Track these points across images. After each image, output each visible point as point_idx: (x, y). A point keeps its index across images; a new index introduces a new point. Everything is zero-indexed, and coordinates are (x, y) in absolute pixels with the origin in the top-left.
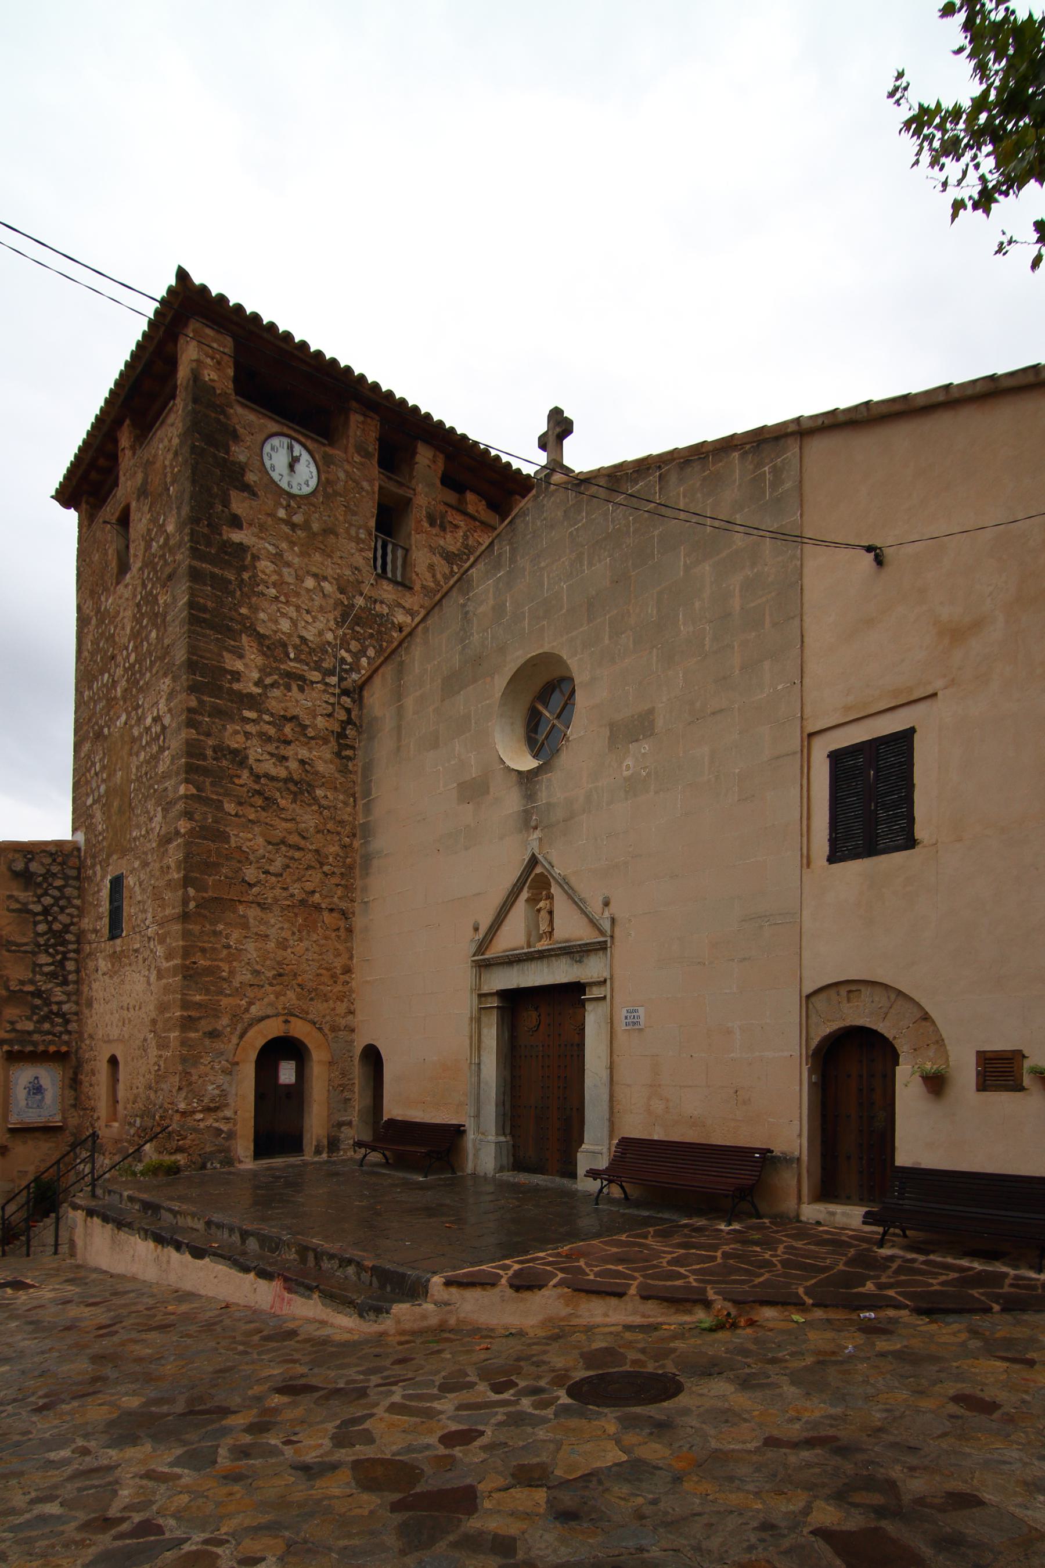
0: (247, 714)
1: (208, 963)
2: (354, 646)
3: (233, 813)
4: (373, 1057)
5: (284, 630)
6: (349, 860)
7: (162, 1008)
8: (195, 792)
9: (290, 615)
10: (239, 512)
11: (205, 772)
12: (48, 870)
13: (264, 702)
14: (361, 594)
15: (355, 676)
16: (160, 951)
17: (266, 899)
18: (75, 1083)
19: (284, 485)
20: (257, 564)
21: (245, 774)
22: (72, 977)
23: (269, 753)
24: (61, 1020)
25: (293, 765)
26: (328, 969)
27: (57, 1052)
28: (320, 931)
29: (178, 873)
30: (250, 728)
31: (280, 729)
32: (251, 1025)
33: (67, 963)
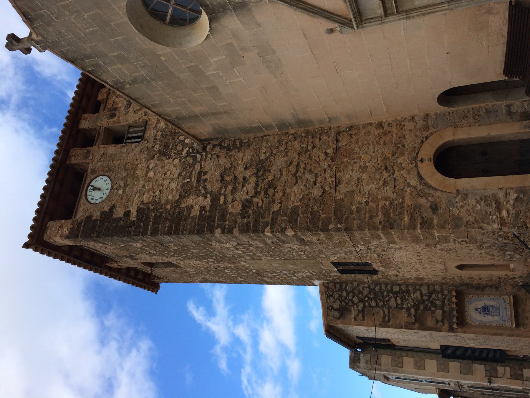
0: (222, 201)
1: (380, 215)
2: (179, 147)
3: (280, 205)
4: (449, 97)
5: (176, 185)
6: (303, 135)
7: (416, 240)
8: (269, 228)
9: (168, 183)
10: (123, 213)
11: (257, 222)
12: (338, 299)
13: (215, 193)
14: (153, 147)
15: (195, 145)
16: (375, 243)
17: (332, 182)
18: (479, 288)
19: (108, 192)
20: (146, 202)
21: (255, 200)
22: (404, 288)
23: (242, 188)
24: (434, 295)
25: (248, 173)
26: (380, 138)
27: (456, 297)
28: (353, 146)
29: (320, 234)
30: (229, 199)
31: (228, 183)
32: (426, 184)
33: (394, 290)
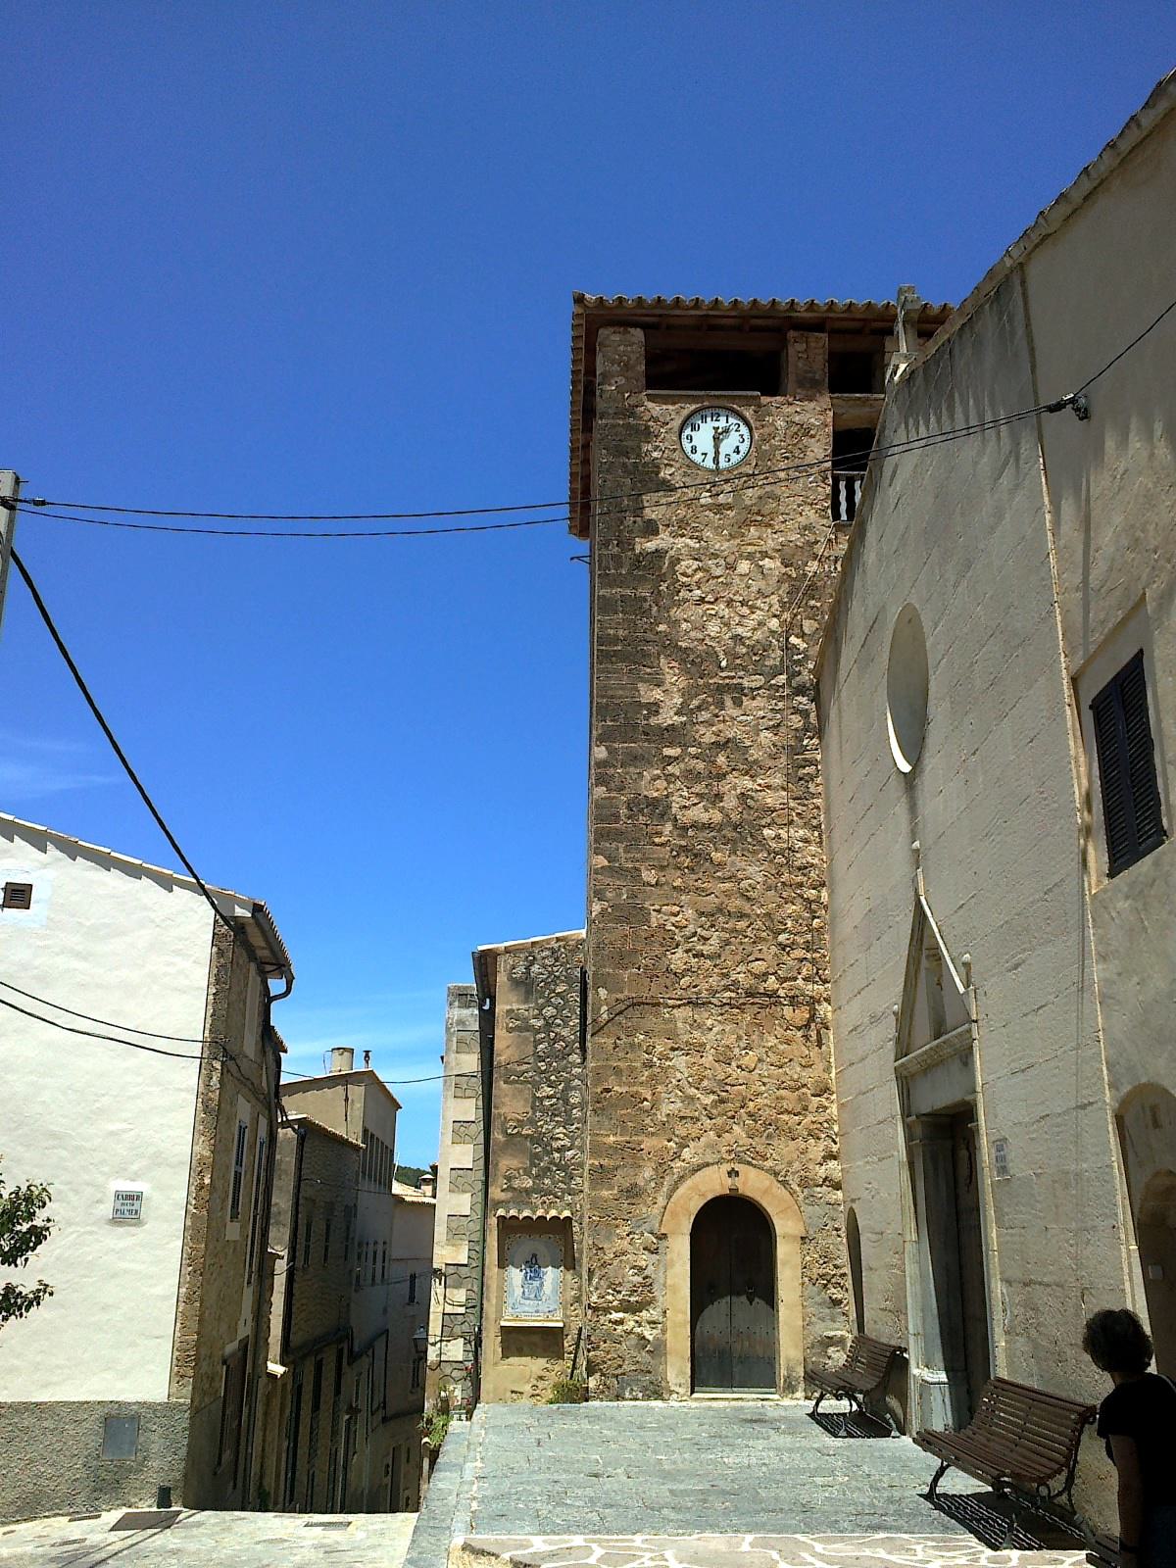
3: (654, 882)
21: (669, 827)
32: (682, 1178)
